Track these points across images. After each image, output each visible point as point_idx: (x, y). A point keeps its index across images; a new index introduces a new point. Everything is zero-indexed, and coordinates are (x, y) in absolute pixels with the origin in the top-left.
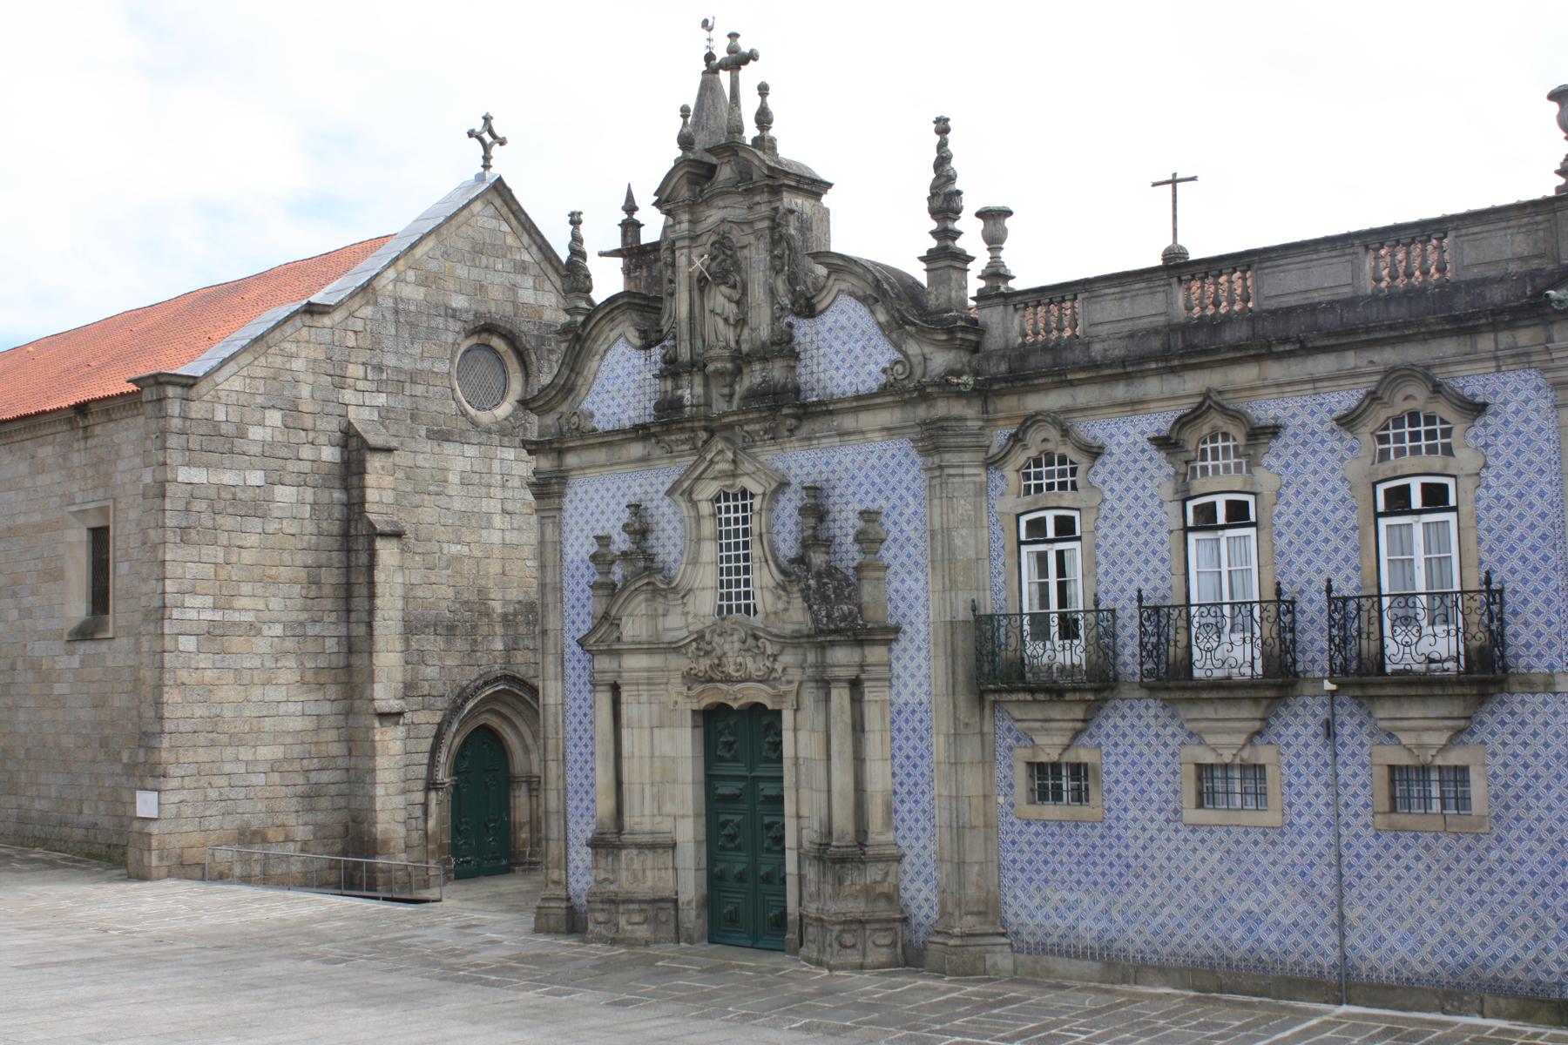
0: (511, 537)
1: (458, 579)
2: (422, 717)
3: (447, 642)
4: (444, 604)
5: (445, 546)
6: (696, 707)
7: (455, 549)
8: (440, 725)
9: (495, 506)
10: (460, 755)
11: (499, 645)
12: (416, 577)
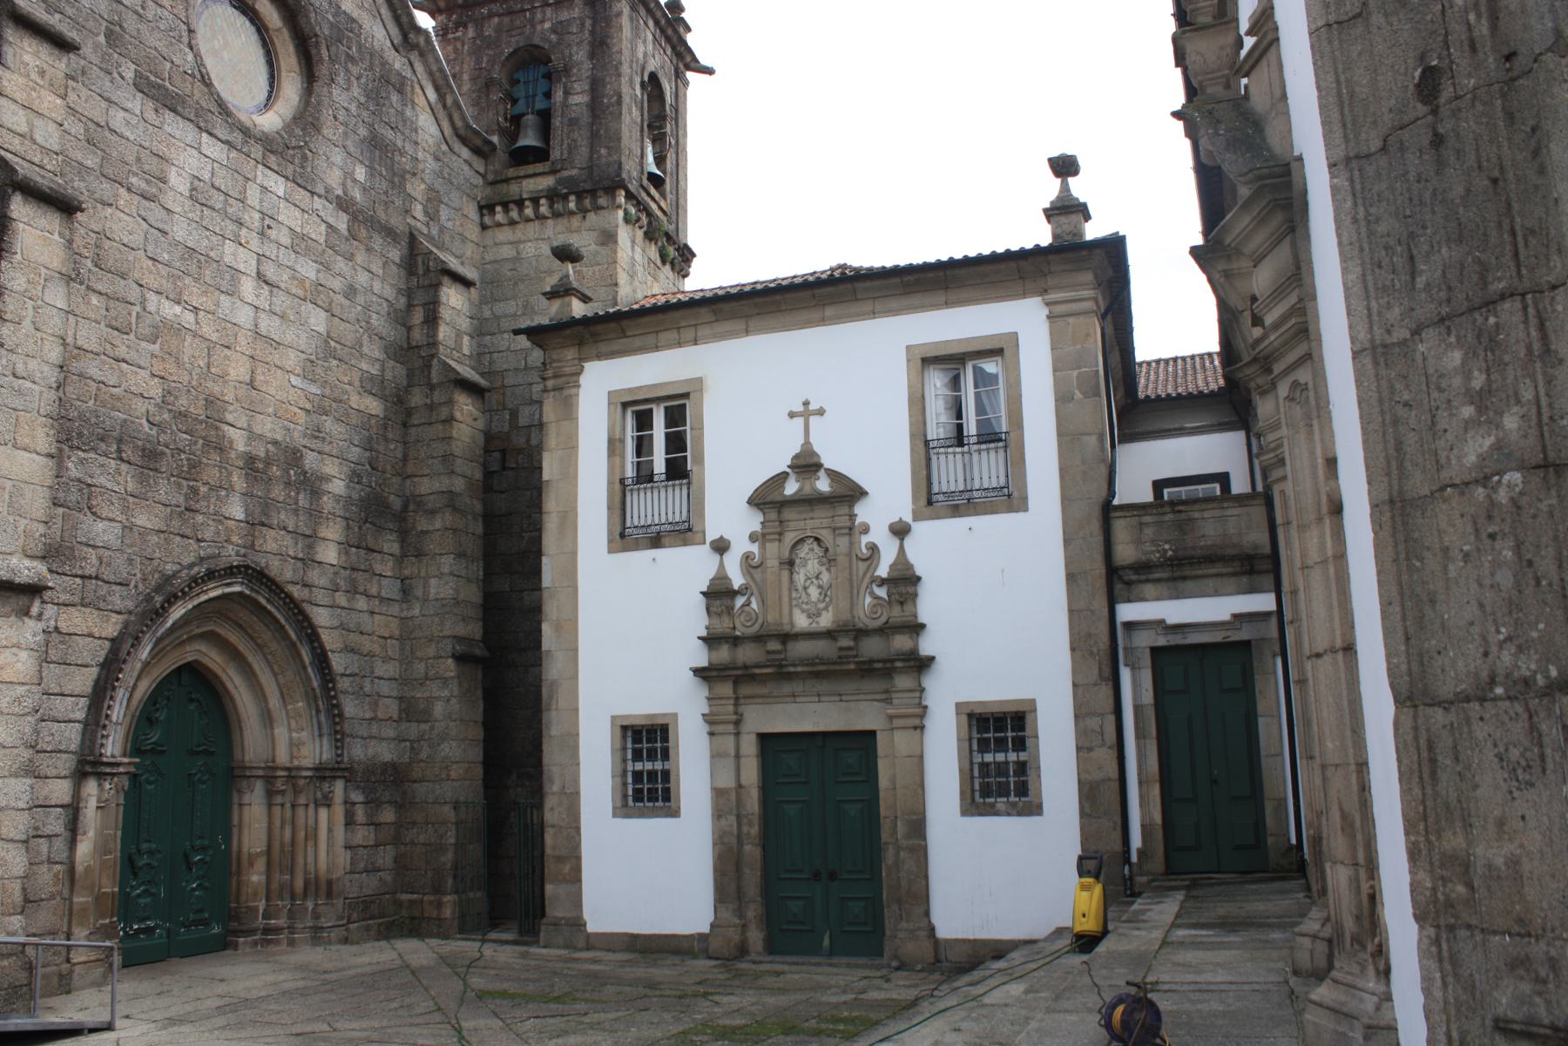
0: (268, 324)
1: (171, 366)
2: (76, 620)
3: (142, 480)
4: (140, 407)
5: (152, 297)
7: (171, 310)
8: (115, 642)
9: (245, 261)
10: (145, 718)
11: (237, 511)
12: (88, 336)
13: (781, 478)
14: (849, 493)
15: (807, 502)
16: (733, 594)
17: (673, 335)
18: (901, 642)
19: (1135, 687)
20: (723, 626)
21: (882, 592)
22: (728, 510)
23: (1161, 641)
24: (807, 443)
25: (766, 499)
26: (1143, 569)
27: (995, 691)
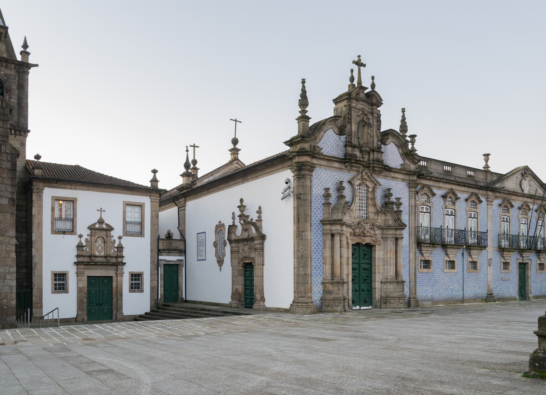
6: (353, 243)
13: (96, 223)
14: (110, 228)
15: (100, 229)
16: (85, 246)
17: (70, 186)
18: (120, 260)
19: (161, 270)
20: (81, 253)
21: (116, 250)
22: (82, 229)
23: (165, 263)
24: (101, 217)
25: (91, 228)
26: (164, 250)
27: (136, 270)
